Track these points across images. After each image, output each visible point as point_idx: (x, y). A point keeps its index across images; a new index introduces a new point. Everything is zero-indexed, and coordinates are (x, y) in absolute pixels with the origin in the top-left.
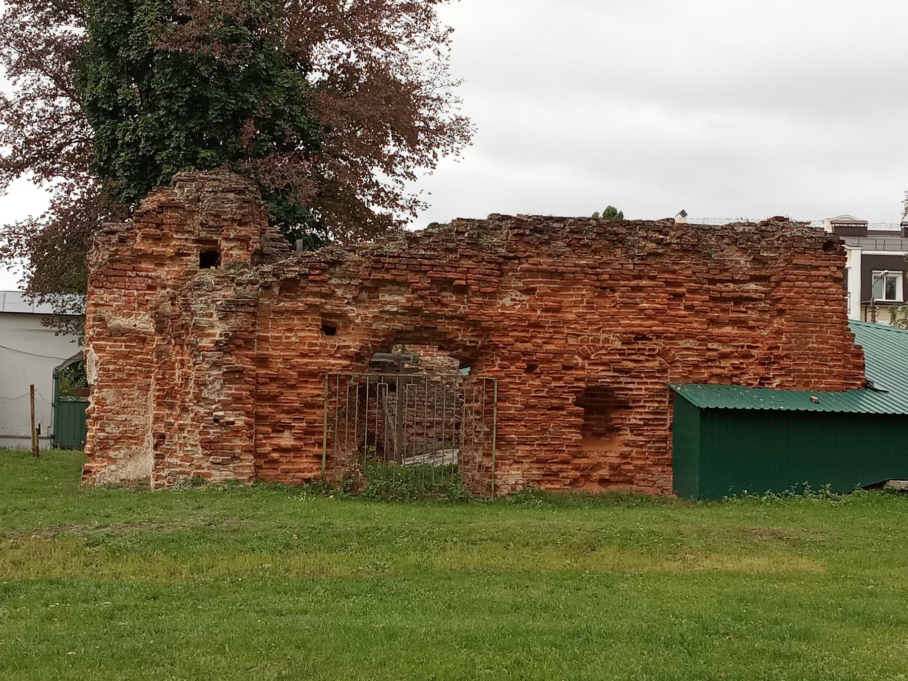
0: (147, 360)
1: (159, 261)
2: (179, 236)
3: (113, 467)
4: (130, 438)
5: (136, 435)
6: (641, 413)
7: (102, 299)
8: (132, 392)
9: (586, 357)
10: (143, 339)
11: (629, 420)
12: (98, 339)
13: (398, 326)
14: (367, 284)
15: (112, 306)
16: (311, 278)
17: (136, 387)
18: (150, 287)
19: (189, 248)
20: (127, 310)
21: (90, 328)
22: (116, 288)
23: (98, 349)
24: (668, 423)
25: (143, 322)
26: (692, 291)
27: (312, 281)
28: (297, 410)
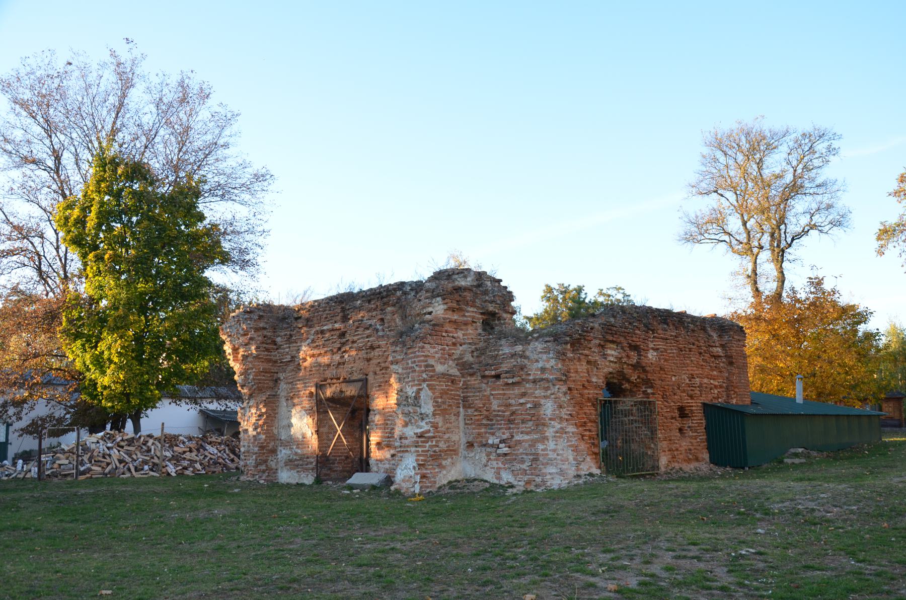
2: (472, 309)
3: (444, 472)
4: (451, 450)
12: (431, 380)
18: (454, 344)
19: (478, 319)
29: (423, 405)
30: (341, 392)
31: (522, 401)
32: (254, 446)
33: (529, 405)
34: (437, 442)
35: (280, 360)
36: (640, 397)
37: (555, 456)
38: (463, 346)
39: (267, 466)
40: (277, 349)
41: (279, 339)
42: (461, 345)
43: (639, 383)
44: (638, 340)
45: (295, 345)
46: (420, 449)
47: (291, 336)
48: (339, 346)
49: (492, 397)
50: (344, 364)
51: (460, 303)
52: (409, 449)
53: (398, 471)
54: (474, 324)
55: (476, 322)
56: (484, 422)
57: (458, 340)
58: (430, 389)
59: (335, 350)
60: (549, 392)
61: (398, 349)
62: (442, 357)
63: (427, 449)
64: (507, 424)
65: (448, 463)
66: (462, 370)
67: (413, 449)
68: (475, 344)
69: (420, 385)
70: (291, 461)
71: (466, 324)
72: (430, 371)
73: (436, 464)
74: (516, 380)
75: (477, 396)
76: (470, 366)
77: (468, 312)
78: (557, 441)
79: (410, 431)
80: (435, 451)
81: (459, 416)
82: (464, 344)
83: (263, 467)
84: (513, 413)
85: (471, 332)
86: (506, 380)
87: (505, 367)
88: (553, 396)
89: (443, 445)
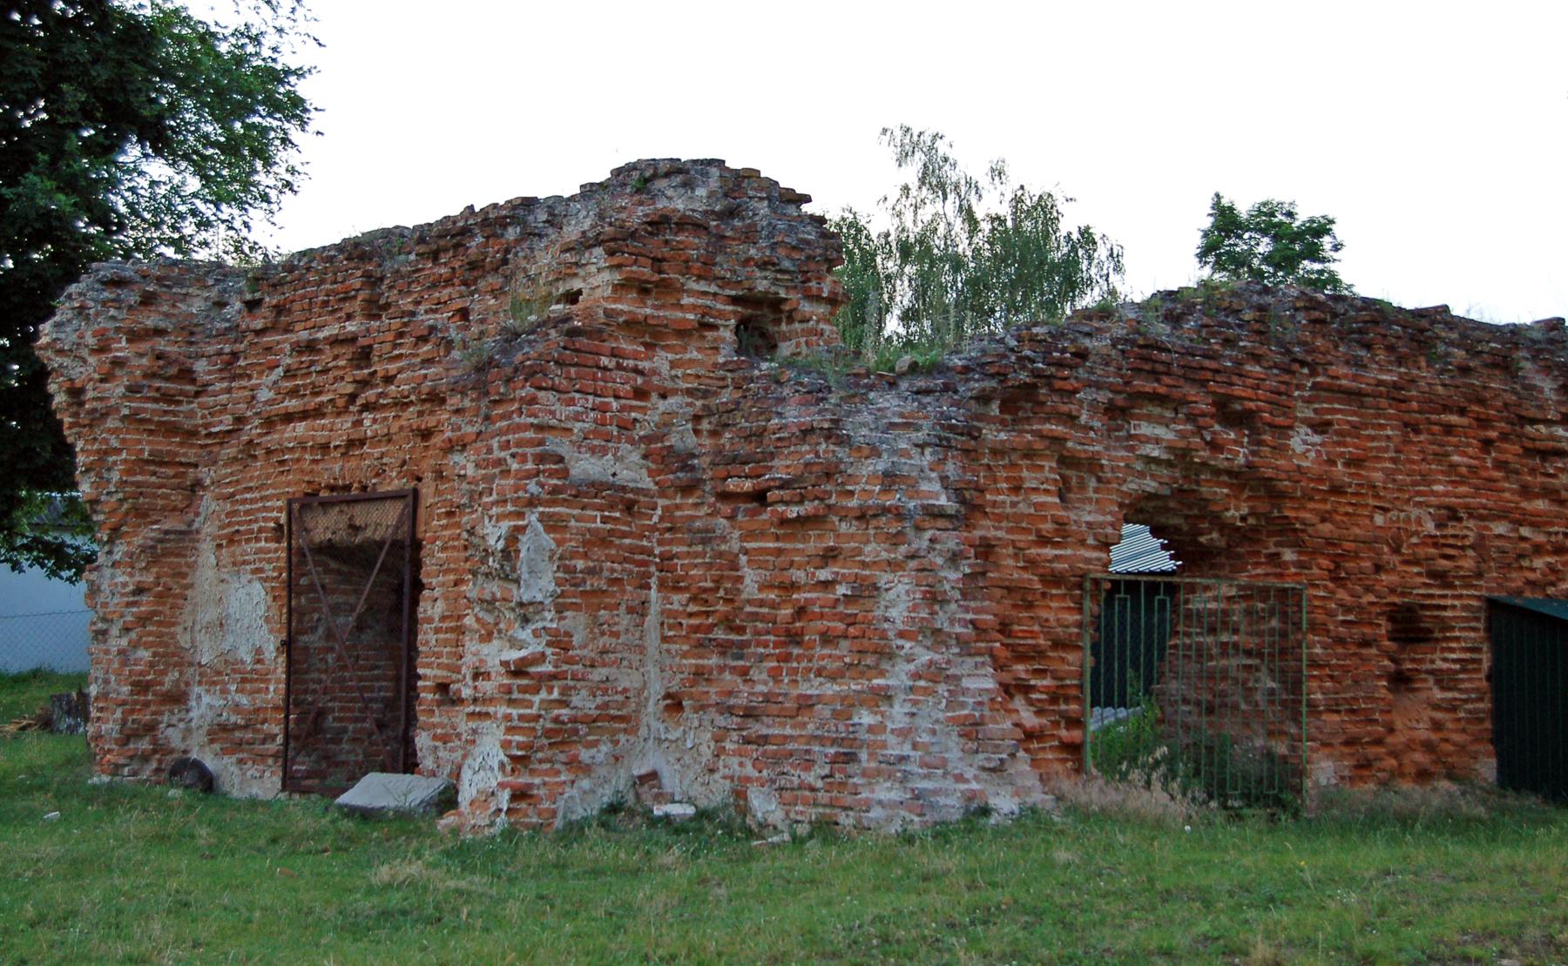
0: (643, 551)
1: (651, 334)
2: (702, 286)
3: (585, 784)
4: (614, 718)
5: (624, 712)
6: (1452, 650)
7: (553, 413)
8: (617, 619)
9: (1396, 550)
10: (628, 503)
11: (1432, 662)
13: (1150, 485)
14: (1120, 400)
15: (570, 430)
16: (1058, 384)
17: (623, 608)
18: (640, 394)
19: (721, 315)
20: (599, 441)
21: (528, 478)
22: (577, 391)
23: (553, 525)
24: (1486, 665)
25: (630, 469)
26: (1504, 437)
27: (1061, 392)
28: (1038, 654)
29: (525, 576)
30: (354, 528)
31: (824, 575)
32: (118, 682)
33: (842, 590)
34: (565, 691)
35: (206, 426)
36: (1255, 573)
37: (906, 750)
38: (671, 400)
39: (155, 742)
40: (197, 394)
41: (201, 366)
42: (664, 396)
43: (1255, 529)
44: (1249, 393)
45: (244, 383)
46: (515, 712)
47: (235, 355)
48: (350, 389)
49: (743, 559)
50: (362, 442)
51: (665, 265)
52: (491, 710)
53: (466, 775)
54: (709, 334)
55: (714, 327)
56: (720, 634)
57: (655, 380)
58: (549, 529)
59: (341, 402)
60: (903, 549)
61: (467, 403)
62: (594, 432)
63: (534, 711)
64: (783, 644)
65: (600, 757)
66: (660, 472)
67: (503, 710)
68: (706, 394)
69: (520, 515)
70: (224, 728)
71: (683, 333)
72: (552, 474)
73: (562, 757)
74: (808, 508)
75: (697, 555)
76: (684, 460)
77: (691, 293)
78: (915, 703)
79: (496, 654)
80: (556, 720)
81: (643, 615)
82: (675, 392)
83: (144, 745)
84: (801, 612)
85: (695, 355)
86: (781, 508)
87: (781, 469)
88: (913, 564)
89: (584, 702)
